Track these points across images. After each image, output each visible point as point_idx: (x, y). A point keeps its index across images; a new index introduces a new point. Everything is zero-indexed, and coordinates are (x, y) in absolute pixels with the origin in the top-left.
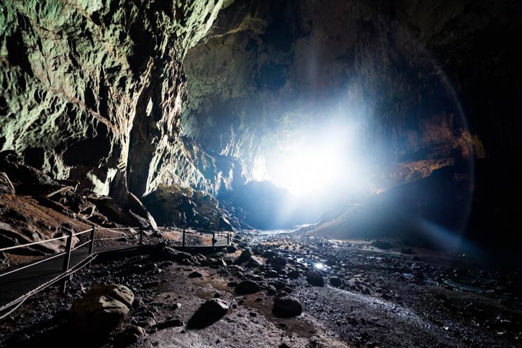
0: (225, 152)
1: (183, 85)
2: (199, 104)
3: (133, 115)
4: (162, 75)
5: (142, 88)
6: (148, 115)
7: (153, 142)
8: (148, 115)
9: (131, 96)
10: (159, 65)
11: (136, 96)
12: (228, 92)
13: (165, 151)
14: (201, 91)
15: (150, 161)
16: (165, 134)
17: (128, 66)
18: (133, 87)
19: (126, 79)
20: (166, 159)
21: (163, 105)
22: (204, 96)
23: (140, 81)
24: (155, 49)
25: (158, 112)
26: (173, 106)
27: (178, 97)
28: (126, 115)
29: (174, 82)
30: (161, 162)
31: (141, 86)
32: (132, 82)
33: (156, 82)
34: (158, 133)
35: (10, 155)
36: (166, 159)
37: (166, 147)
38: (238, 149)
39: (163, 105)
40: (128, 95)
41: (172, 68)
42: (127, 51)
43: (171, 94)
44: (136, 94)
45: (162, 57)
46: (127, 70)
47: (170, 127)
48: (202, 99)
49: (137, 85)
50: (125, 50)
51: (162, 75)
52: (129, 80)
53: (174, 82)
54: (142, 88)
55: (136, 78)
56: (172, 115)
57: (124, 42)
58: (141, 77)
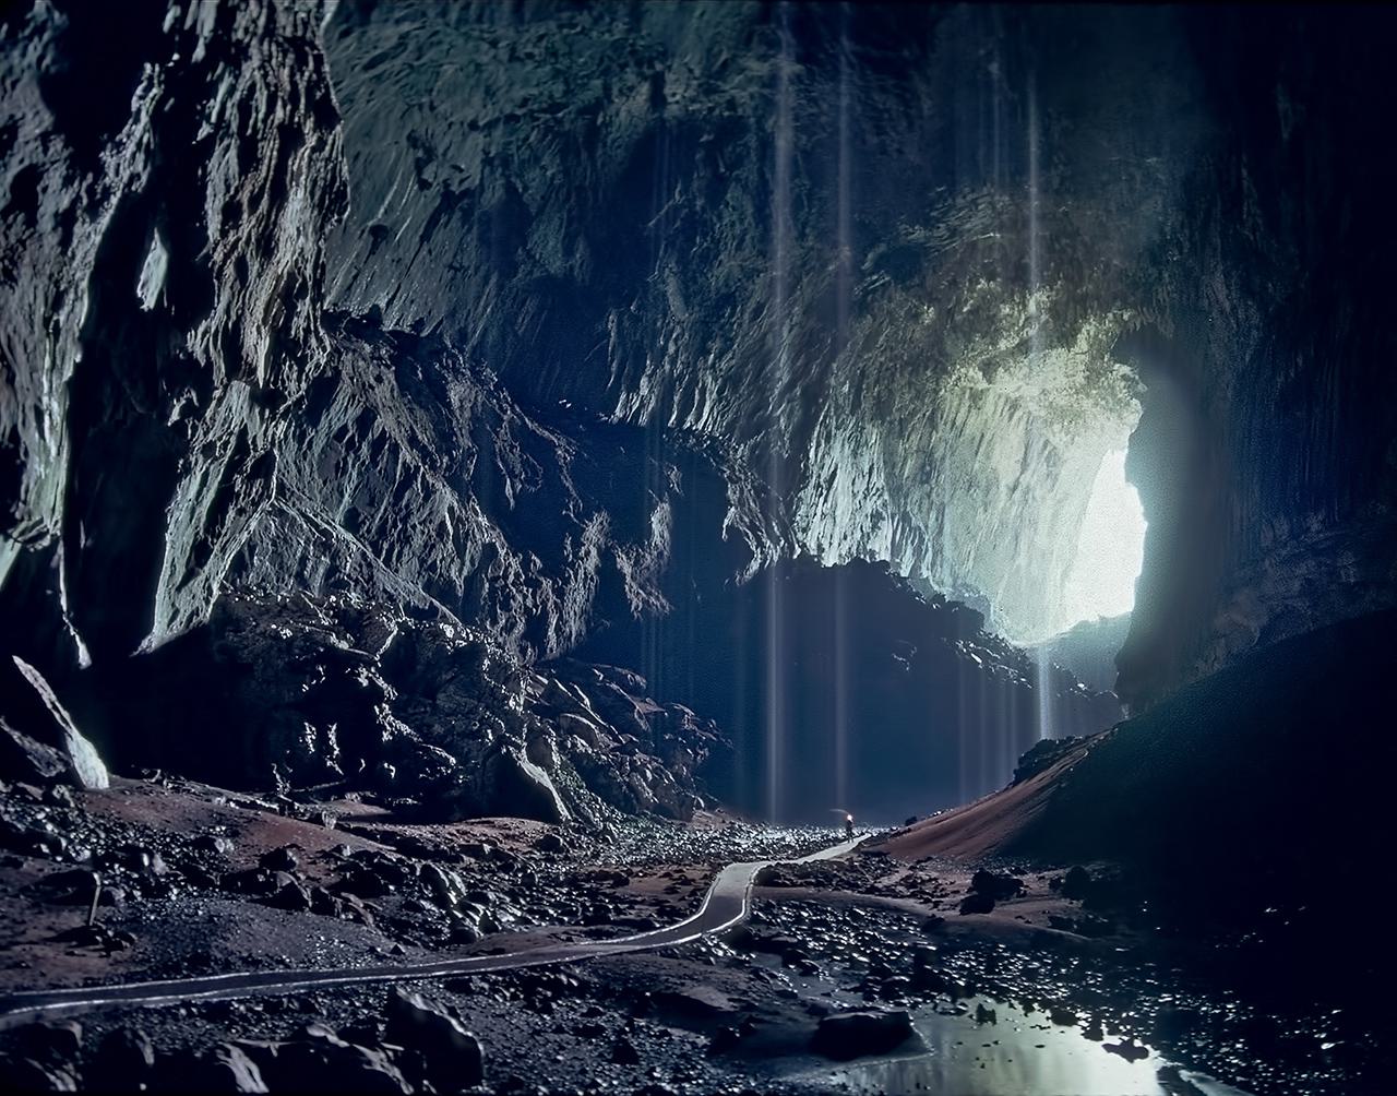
0: (638, 402)
1: (321, 144)
2: (487, 161)
3: (77, 311)
4: (204, 131)
5: (114, 200)
6: (149, 303)
7: (175, 416)
8: (149, 303)
9: (65, 242)
10: (189, 88)
11: (90, 237)
12: (645, 88)
13: (242, 448)
14: (490, 93)
15: (168, 494)
16: (232, 373)
17: (47, 119)
18: (76, 200)
19: (40, 177)
20: (250, 479)
21: (218, 257)
22: (511, 118)
23: (100, 171)
24: (167, 25)
25: (191, 288)
26: (266, 245)
27: (297, 202)
28: (46, 321)
29: (269, 150)
30: (225, 496)
31: (107, 192)
32: (67, 182)
33: (179, 159)
34: (200, 378)
35: (60, 894)
36: (250, 479)
37: (243, 432)
38: (712, 387)
39: (218, 257)
40: (52, 240)
41: (252, 89)
42: (41, 59)
43: (254, 201)
44: (88, 228)
45: (199, 53)
46: (45, 138)
47: (257, 345)
48: (498, 133)
49: (91, 191)
50: (32, 55)
51: (204, 131)
52: (54, 179)
53: (269, 150)
54: (114, 200)
55: (85, 162)
56: (262, 291)
57: (26, 24)
58: (105, 156)
